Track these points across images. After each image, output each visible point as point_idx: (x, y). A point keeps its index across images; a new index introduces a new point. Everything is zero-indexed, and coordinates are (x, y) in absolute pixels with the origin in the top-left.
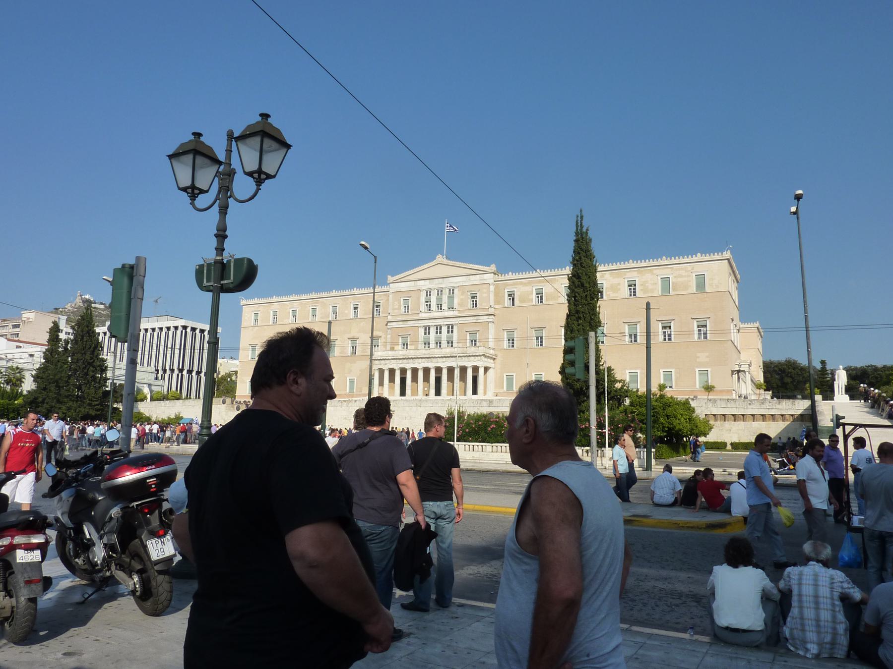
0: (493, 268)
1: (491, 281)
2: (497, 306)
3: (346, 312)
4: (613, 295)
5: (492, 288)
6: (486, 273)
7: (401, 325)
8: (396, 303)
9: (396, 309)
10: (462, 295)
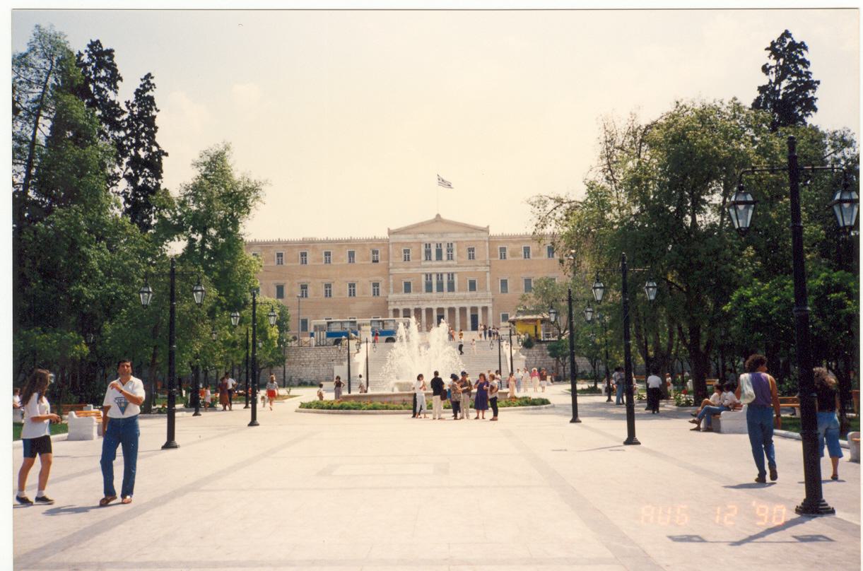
5: (487, 244)
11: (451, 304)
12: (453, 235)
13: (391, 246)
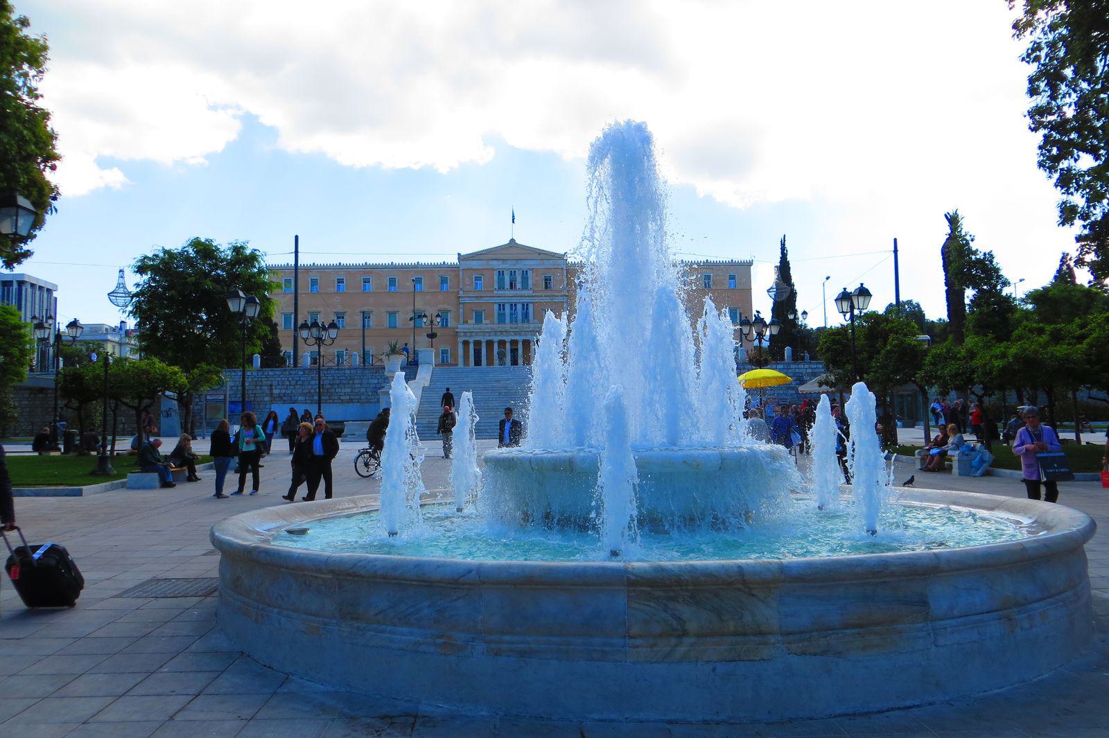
9: (467, 285)
10: (537, 276)
12: (527, 262)
13: (461, 273)
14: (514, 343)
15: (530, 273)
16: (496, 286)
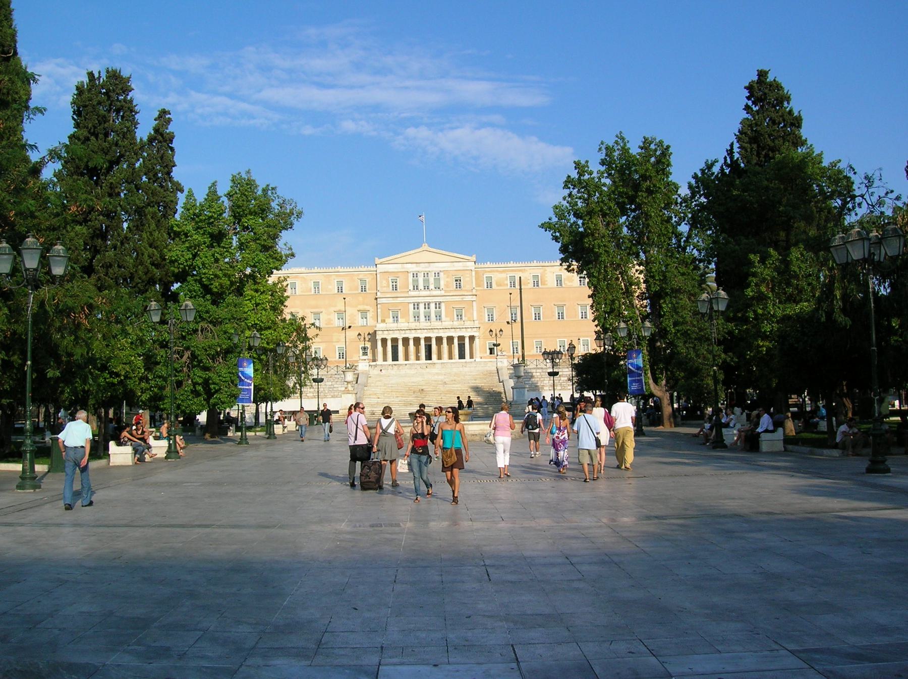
0: (474, 258)
1: (473, 268)
2: (477, 288)
3: (330, 287)
4: (569, 284)
5: (474, 273)
6: (468, 260)
7: (391, 301)
8: (384, 282)
9: (384, 287)
10: (448, 277)
11: (438, 333)
13: (378, 275)
14: (428, 339)
15: (442, 274)
16: (411, 287)
